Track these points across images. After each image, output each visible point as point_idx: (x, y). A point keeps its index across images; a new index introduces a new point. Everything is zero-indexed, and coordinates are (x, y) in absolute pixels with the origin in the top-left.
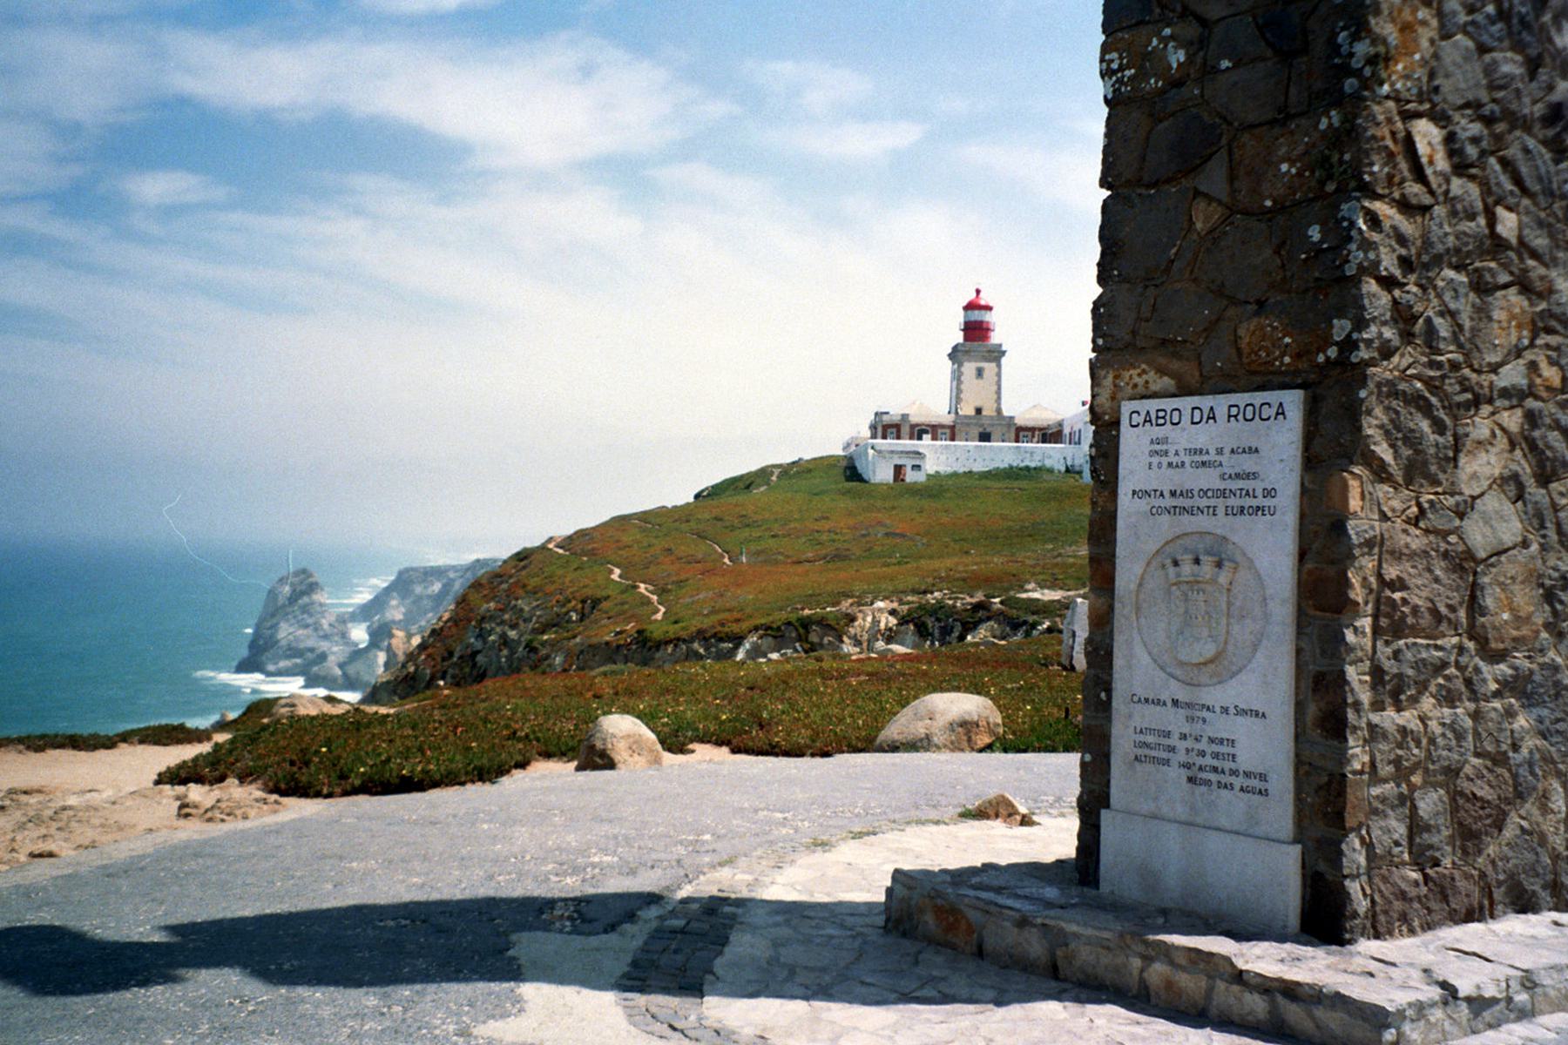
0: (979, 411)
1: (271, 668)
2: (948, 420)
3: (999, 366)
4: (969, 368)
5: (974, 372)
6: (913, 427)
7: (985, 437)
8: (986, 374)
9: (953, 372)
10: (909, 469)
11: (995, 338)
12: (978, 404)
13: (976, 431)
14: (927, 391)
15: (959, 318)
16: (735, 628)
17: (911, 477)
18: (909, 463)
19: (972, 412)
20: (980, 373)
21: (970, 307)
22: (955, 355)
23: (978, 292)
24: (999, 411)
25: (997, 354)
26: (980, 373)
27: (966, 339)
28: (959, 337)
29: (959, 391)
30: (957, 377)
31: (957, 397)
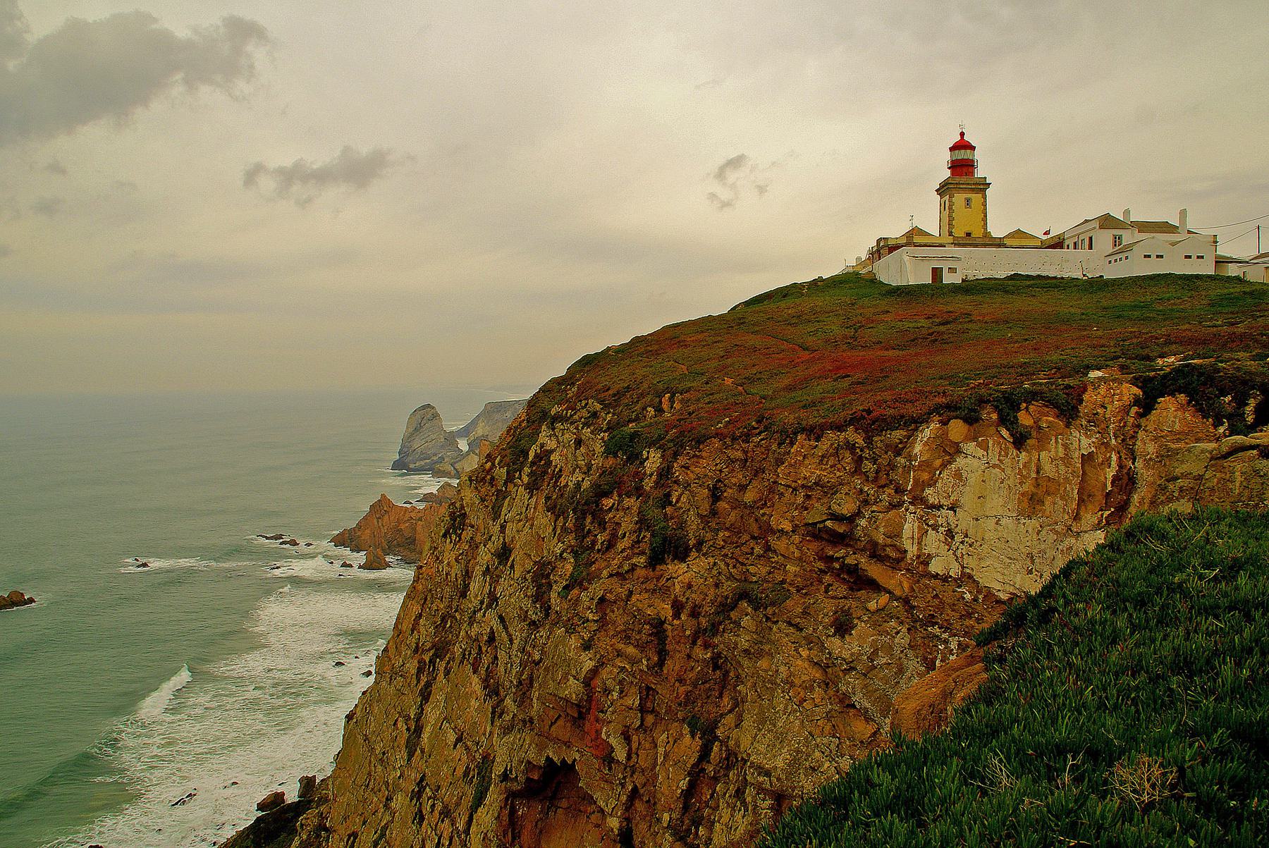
1: (412, 466)
3: (985, 197)
4: (959, 198)
5: (963, 203)
9: (943, 206)
10: (945, 272)
11: (980, 172)
12: (968, 230)
15: (947, 156)
16: (912, 410)
17: (948, 279)
18: (945, 266)
19: (963, 235)
20: (968, 201)
22: (943, 189)
23: (962, 134)
25: (982, 186)
28: (948, 173)
29: (951, 219)
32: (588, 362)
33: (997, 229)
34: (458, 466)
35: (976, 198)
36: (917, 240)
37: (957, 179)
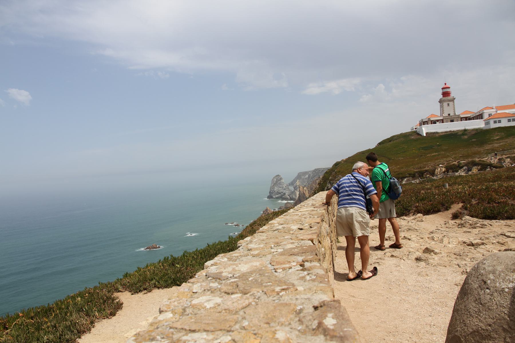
0: (449, 115)
2: (441, 118)
3: (454, 102)
4: (445, 104)
5: (447, 105)
6: (432, 121)
7: (452, 121)
8: (450, 105)
11: (452, 95)
13: (449, 120)
14: (434, 110)
15: (441, 91)
20: (448, 105)
21: (443, 89)
22: (441, 101)
23: (445, 84)
24: (455, 114)
25: (453, 100)
26: (448, 105)
27: (443, 97)
29: (443, 110)
30: (442, 107)
31: (442, 112)
32: (337, 164)
33: (459, 111)
34: (291, 196)
35: (451, 103)
36: (432, 119)
37: (444, 98)
